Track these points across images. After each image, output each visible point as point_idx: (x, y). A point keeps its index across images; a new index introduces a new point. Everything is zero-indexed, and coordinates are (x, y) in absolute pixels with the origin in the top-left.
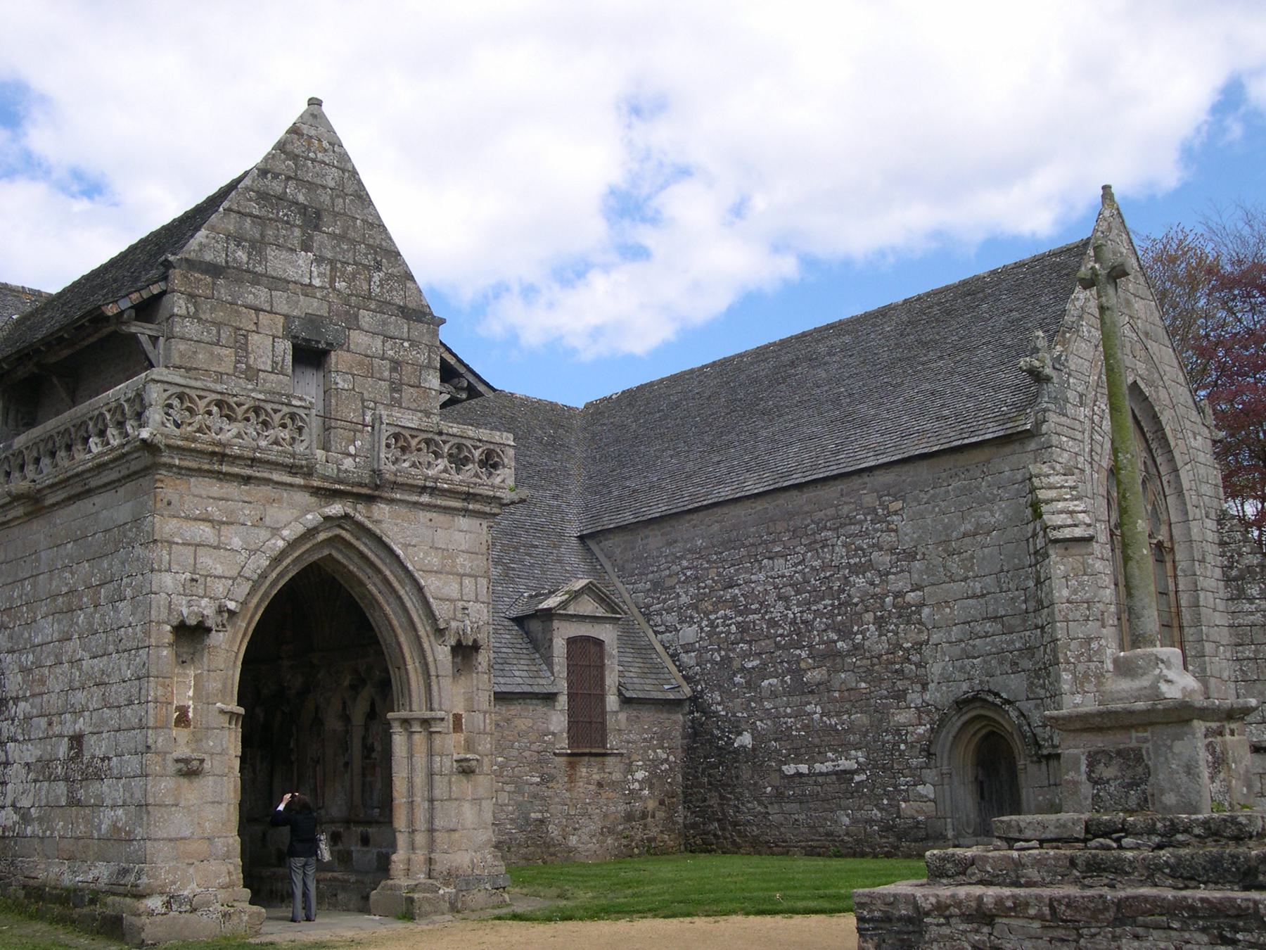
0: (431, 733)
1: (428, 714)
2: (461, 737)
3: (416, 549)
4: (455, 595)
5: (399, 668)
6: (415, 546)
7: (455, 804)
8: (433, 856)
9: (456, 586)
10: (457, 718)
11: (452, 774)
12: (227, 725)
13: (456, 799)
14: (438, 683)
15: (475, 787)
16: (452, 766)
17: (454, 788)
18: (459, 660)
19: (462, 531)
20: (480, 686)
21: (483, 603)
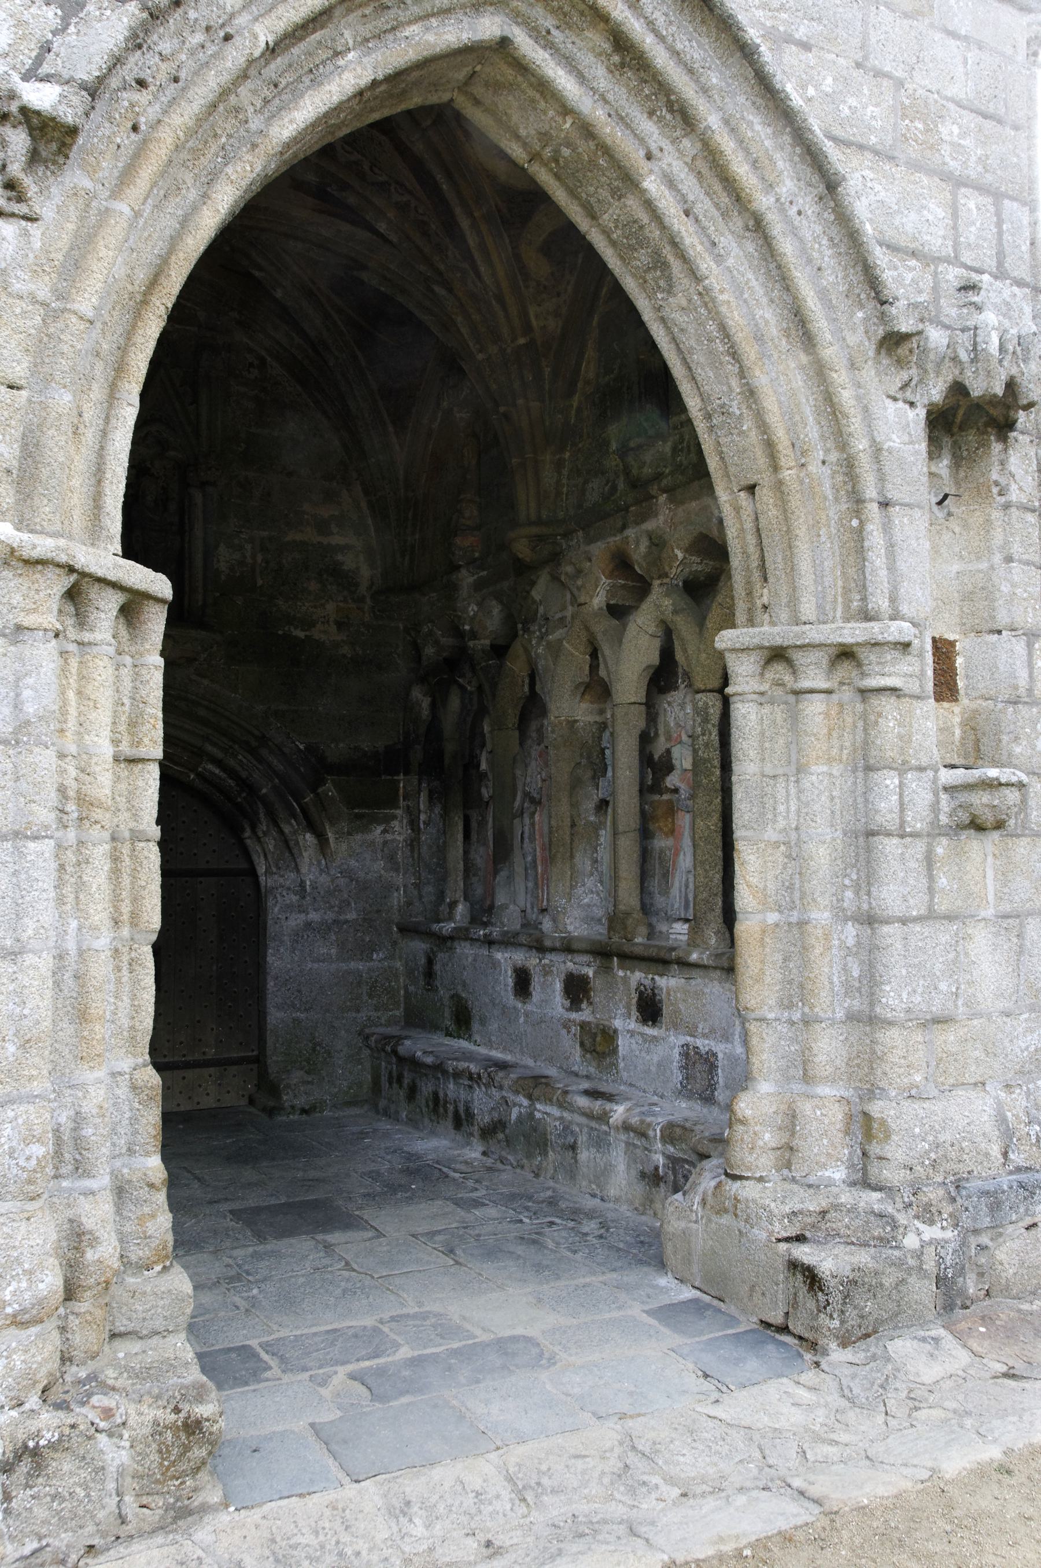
0: (864, 693)
1: (852, 633)
2: (954, 713)
3: (810, 57)
4: (936, 241)
5: (751, 489)
6: (806, 46)
7: (945, 934)
8: (876, 1109)
9: (936, 211)
10: (943, 651)
11: (936, 831)
12: (50, 620)
13: (950, 918)
14: (887, 528)
15: (1004, 877)
16: (935, 808)
17: (943, 881)
18: (943, 467)
19: (953, 34)
20: (1016, 549)
21: (1019, 283)
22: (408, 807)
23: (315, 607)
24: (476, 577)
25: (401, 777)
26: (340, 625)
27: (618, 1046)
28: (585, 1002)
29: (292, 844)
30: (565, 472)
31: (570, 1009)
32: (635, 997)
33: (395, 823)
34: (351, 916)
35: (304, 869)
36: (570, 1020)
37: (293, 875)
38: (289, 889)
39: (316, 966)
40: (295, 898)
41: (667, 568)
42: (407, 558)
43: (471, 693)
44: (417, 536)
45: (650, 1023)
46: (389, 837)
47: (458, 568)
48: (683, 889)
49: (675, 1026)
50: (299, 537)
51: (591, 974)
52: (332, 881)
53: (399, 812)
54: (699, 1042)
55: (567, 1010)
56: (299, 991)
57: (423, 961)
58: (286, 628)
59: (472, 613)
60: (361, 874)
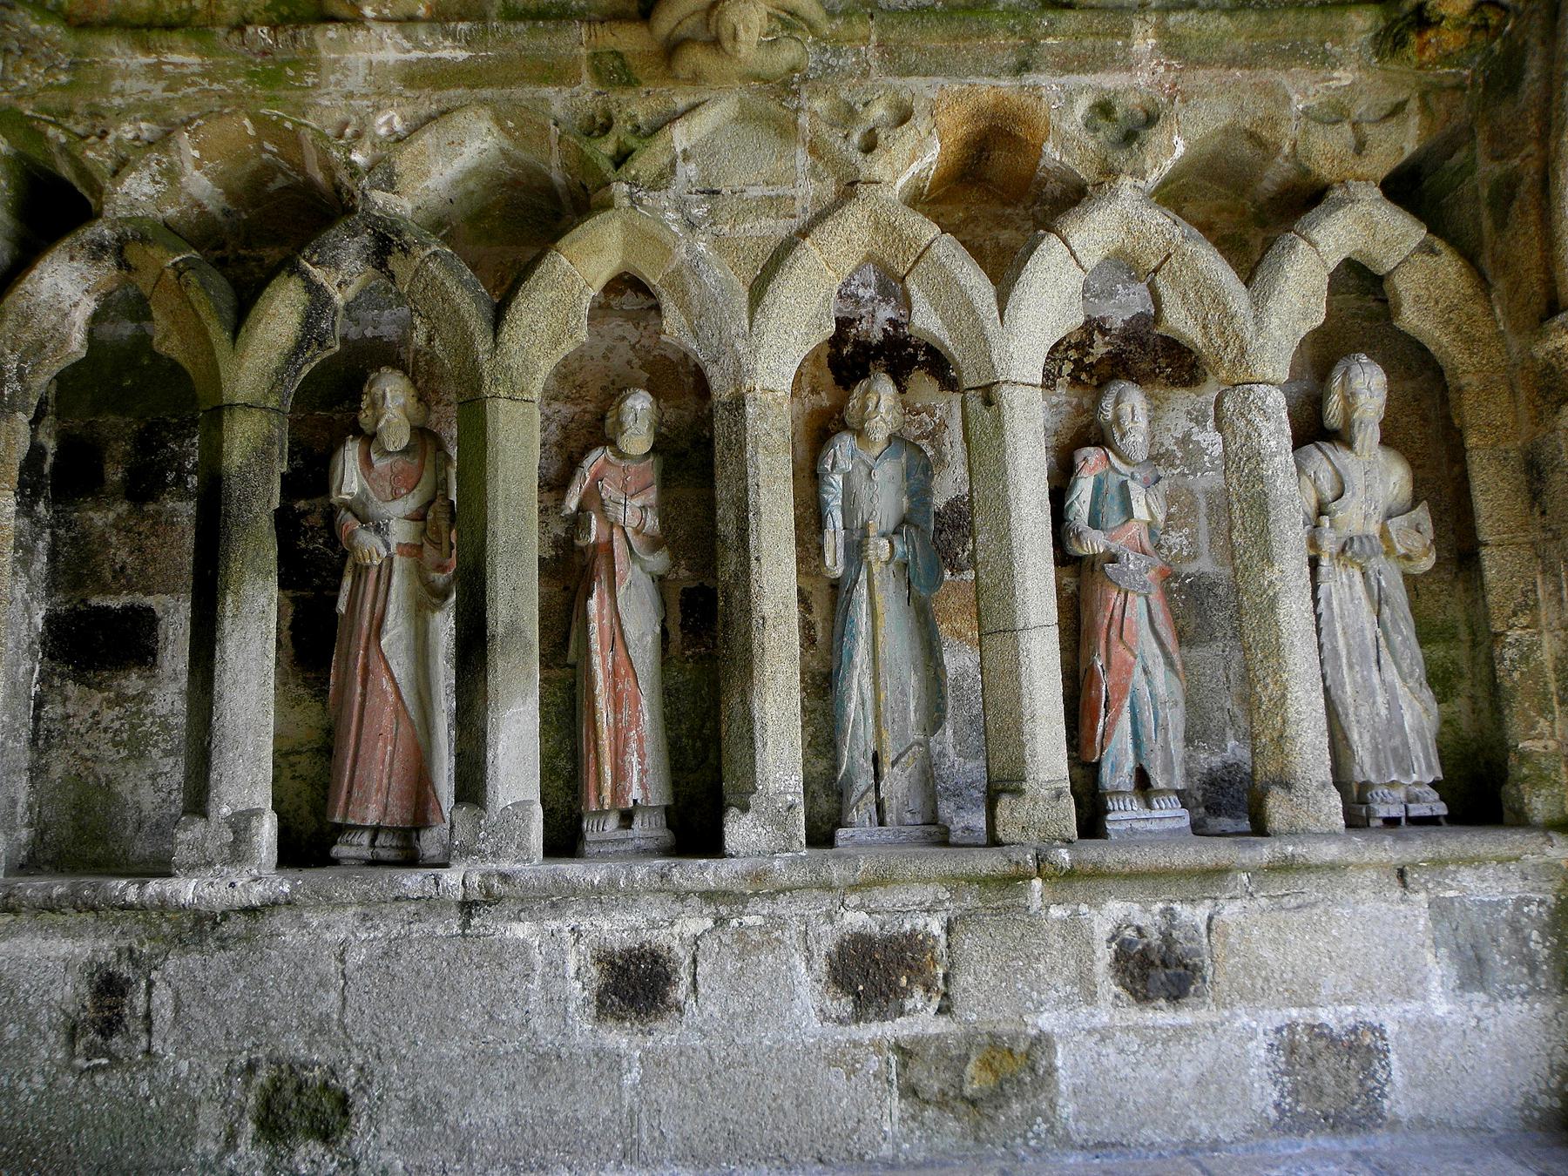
24: (417, 54)
27: (1051, 1070)
28: (919, 992)
31: (857, 1018)
32: (1104, 955)
36: (856, 1044)
41: (1149, 163)
45: (1162, 1002)
49: (1250, 996)
51: (936, 926)
54: (1326, 1015)
55: (841, 1021)
59: (383, 131)
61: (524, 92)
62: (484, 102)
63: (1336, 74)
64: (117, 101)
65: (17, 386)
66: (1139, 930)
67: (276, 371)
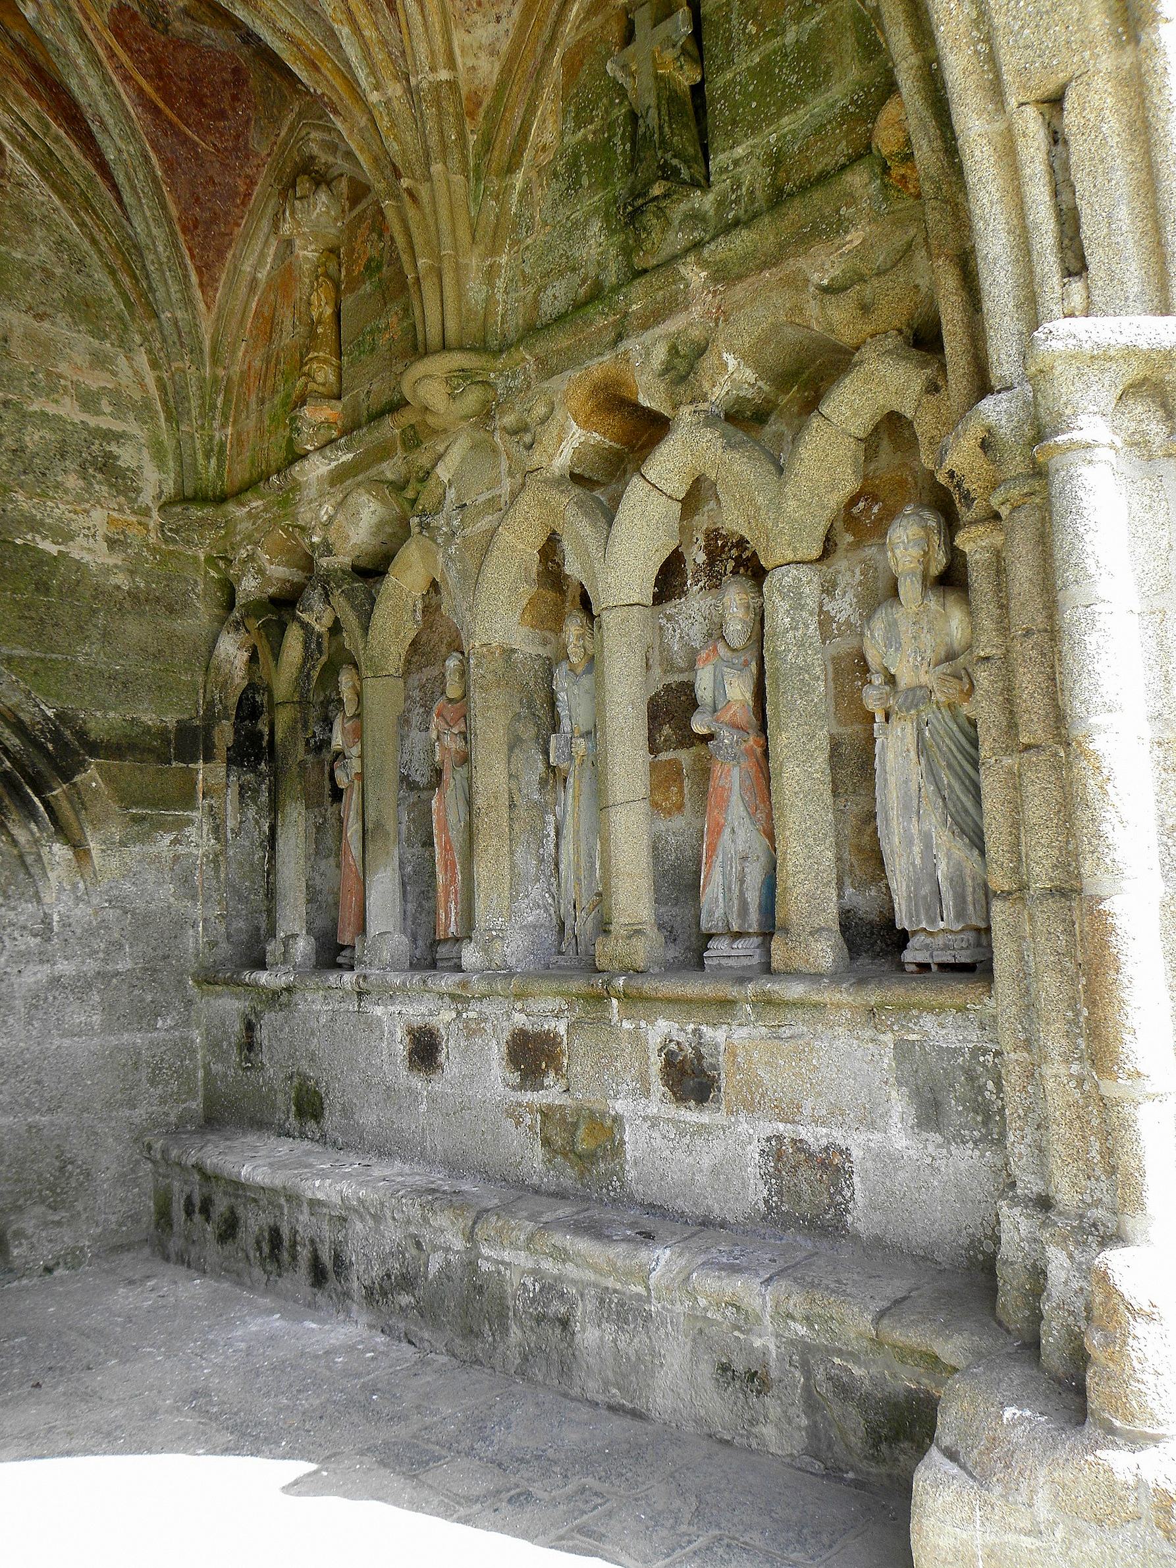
22: (211, 807)
23: (75, 512)
24: (334, 464)
25: (200, 764)
26: (112, 543)
27: (622, 1143)
28: (552, 1074)
29: (29, 859)
30: (500, 283)
31: (521, 1087)
32: (656, 1063)
33: (191, 831)
34: (124, 965)
35: (48, 898)
36: (520, 1105)
37: (30, 907)
38: (24, 928)
39: (67, 1042)
40: (33, 942)
41: (706, 386)
42: (213, 461)
43: (320, 636)
44: (230, 430)
45: (692, 1103)
46: (181, 849)
47: (304, 456)
48: (735, 888)
49: (750, 1107)
50: (51, 409)
51: (562, 1029)
52: (96, 913)
53: (196, 815)
54: (804, 1133)
55: (514, 1088)
56: (38, 1082)
57: (238, 1027)
58: (29, 537)
59: (325, 518)
60: (140, 904)
61: (372, 472)
62: (359, 485)
63: (848, 238)
64: (238, 538)
65: (220, 706)
66: (678, 1043)
67: (296, 679)
